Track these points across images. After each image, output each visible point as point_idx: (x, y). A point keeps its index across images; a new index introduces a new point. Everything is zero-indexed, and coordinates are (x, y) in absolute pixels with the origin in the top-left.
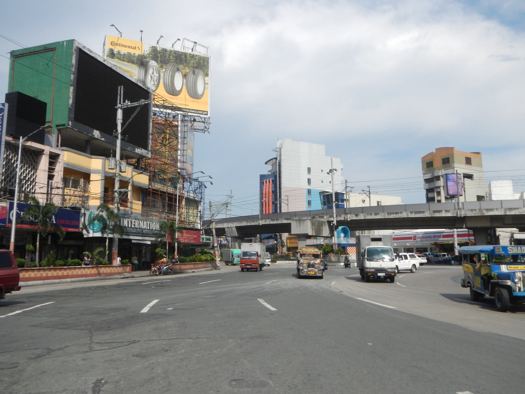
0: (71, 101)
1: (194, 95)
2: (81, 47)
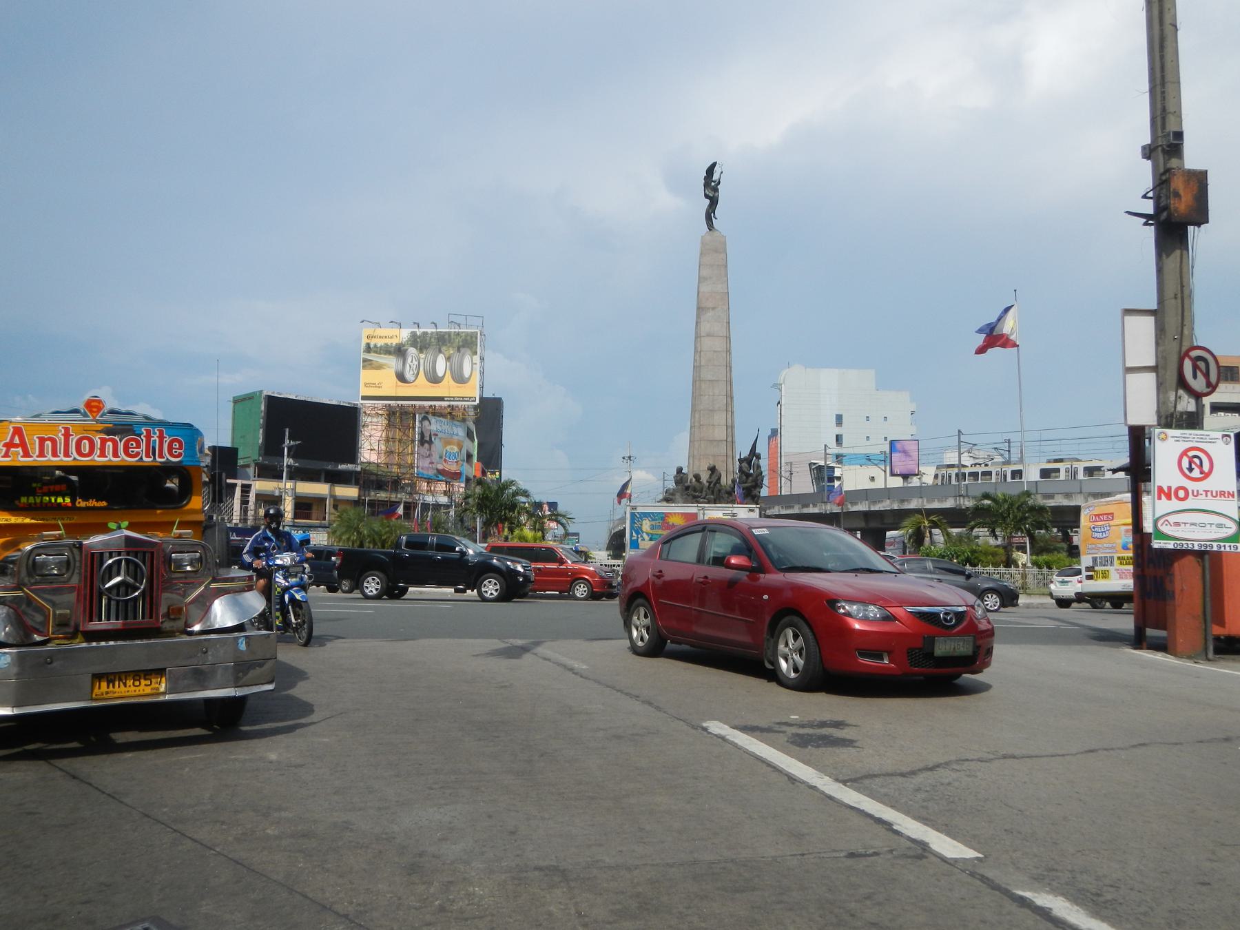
0: (260, 441)
1: (460, 379)
2: (270, 394)
